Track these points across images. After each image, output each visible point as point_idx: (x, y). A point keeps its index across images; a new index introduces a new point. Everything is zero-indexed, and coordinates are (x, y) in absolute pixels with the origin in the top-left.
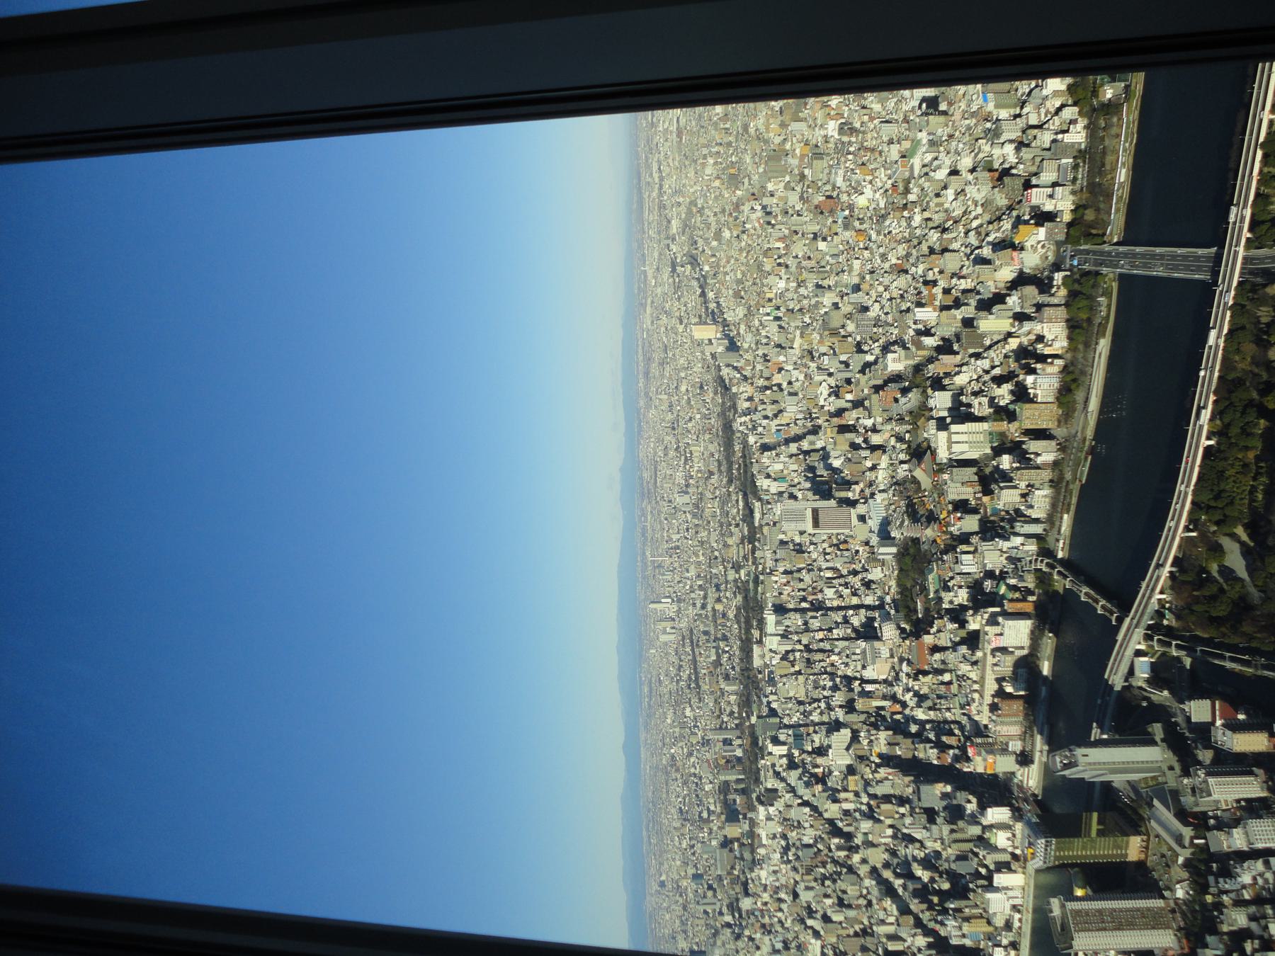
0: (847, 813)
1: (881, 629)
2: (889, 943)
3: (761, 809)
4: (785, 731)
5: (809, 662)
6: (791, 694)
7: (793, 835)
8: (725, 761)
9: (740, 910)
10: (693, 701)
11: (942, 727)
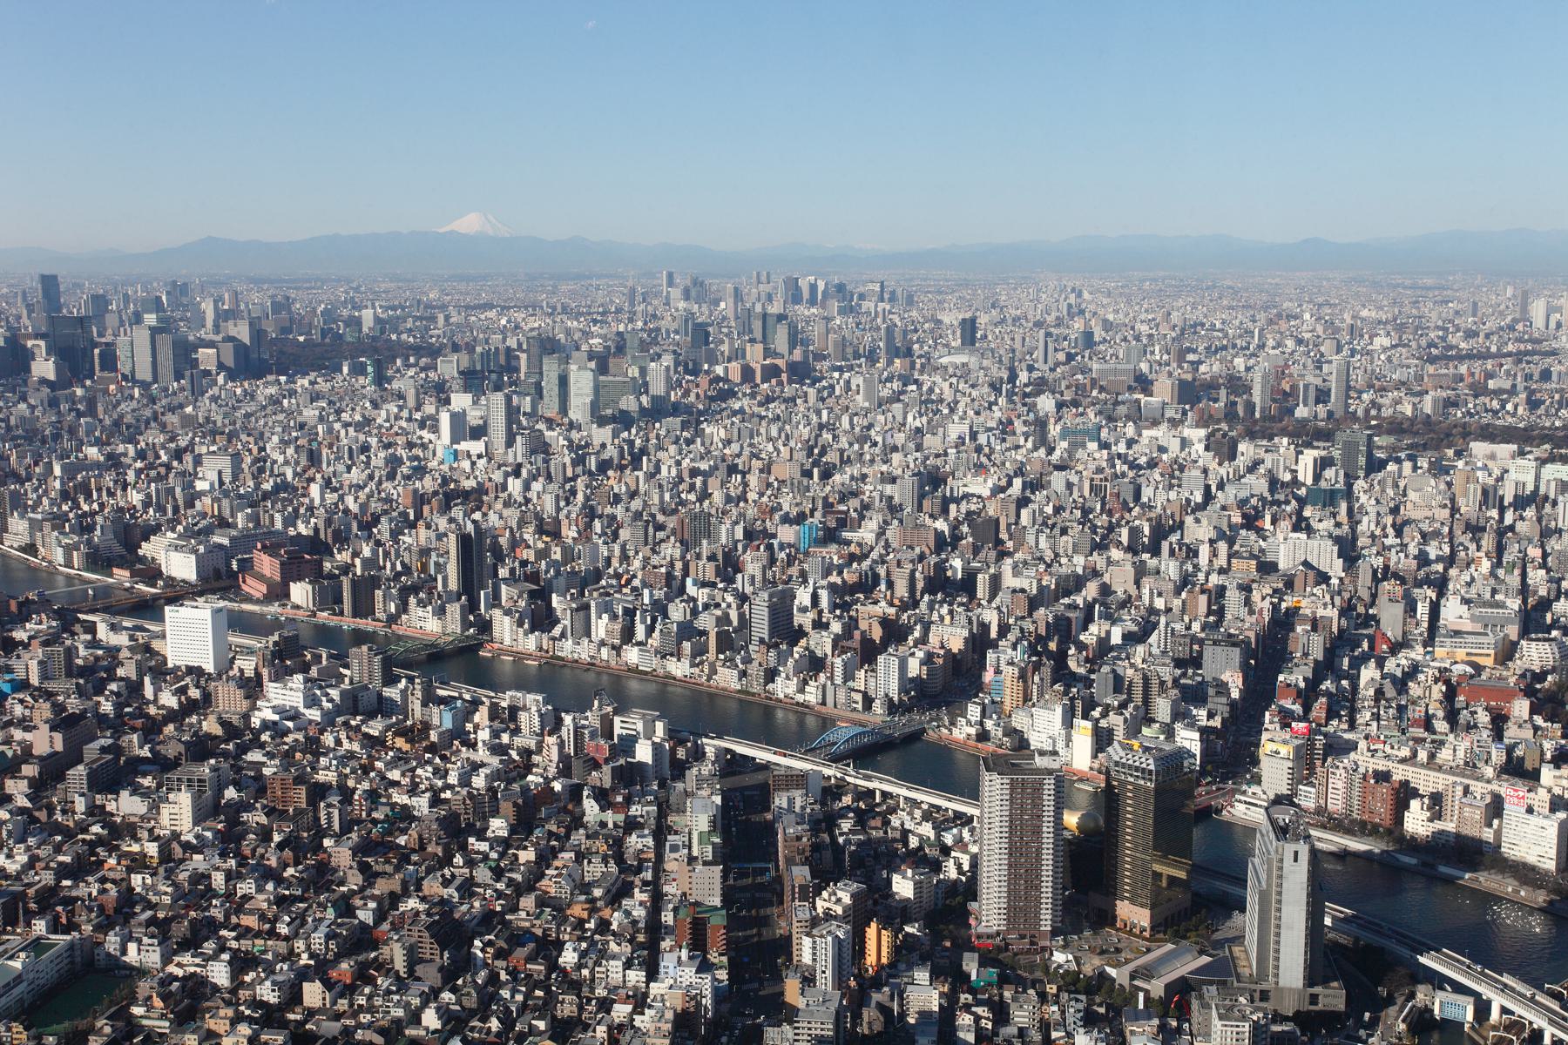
0: (1192, 553)
1: (1545, 640)
2: (987, 577)
3: (1202, 432)
4: (1341, 479)
5: (1475, 530)
6: (1412, 495)
7: (1156, 474)
8: (1288, 389)
9: (1038, 393)
10: (1404, 350)
11: (1343, 705)
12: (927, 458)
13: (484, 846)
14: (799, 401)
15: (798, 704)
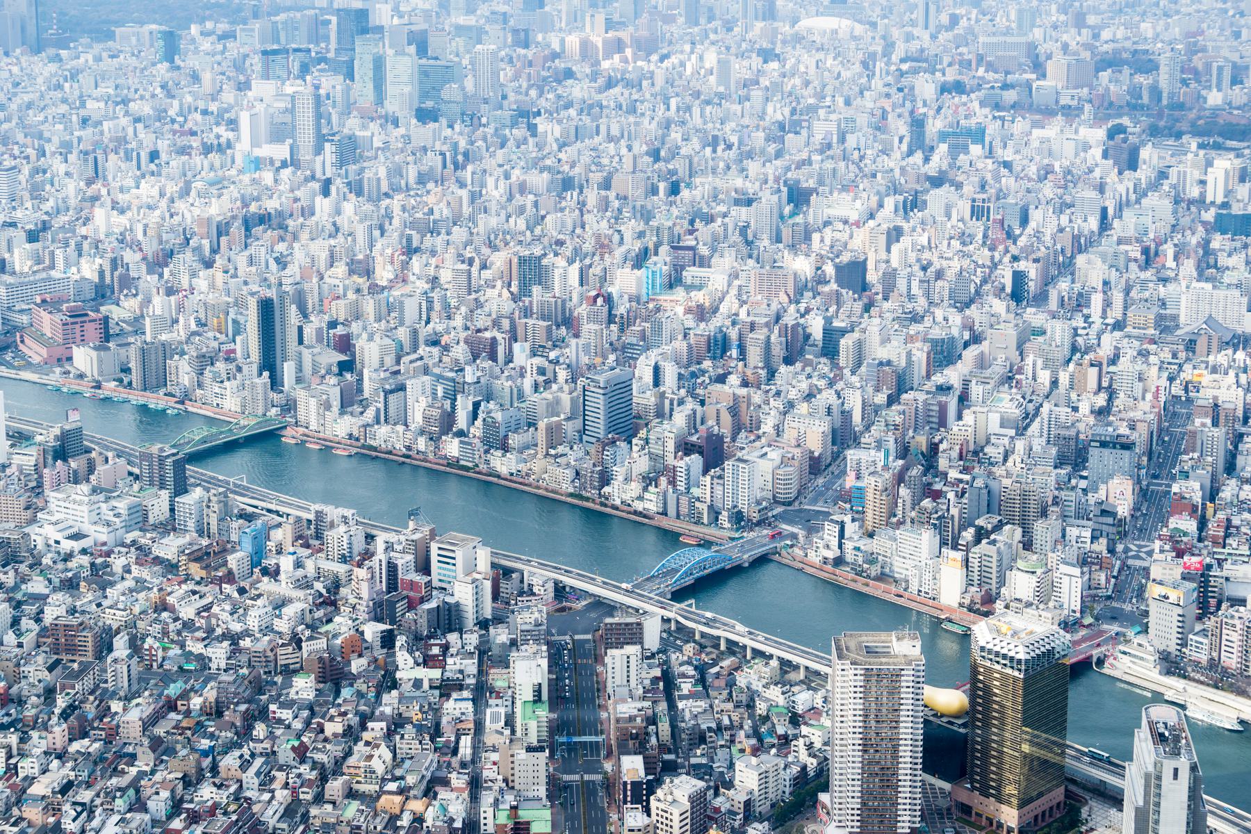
3: (1100, 134)
8: (1200, 67)
12: (788, 169)
13: (286, 715)
14: (645, 83)
15: (635, 513)
